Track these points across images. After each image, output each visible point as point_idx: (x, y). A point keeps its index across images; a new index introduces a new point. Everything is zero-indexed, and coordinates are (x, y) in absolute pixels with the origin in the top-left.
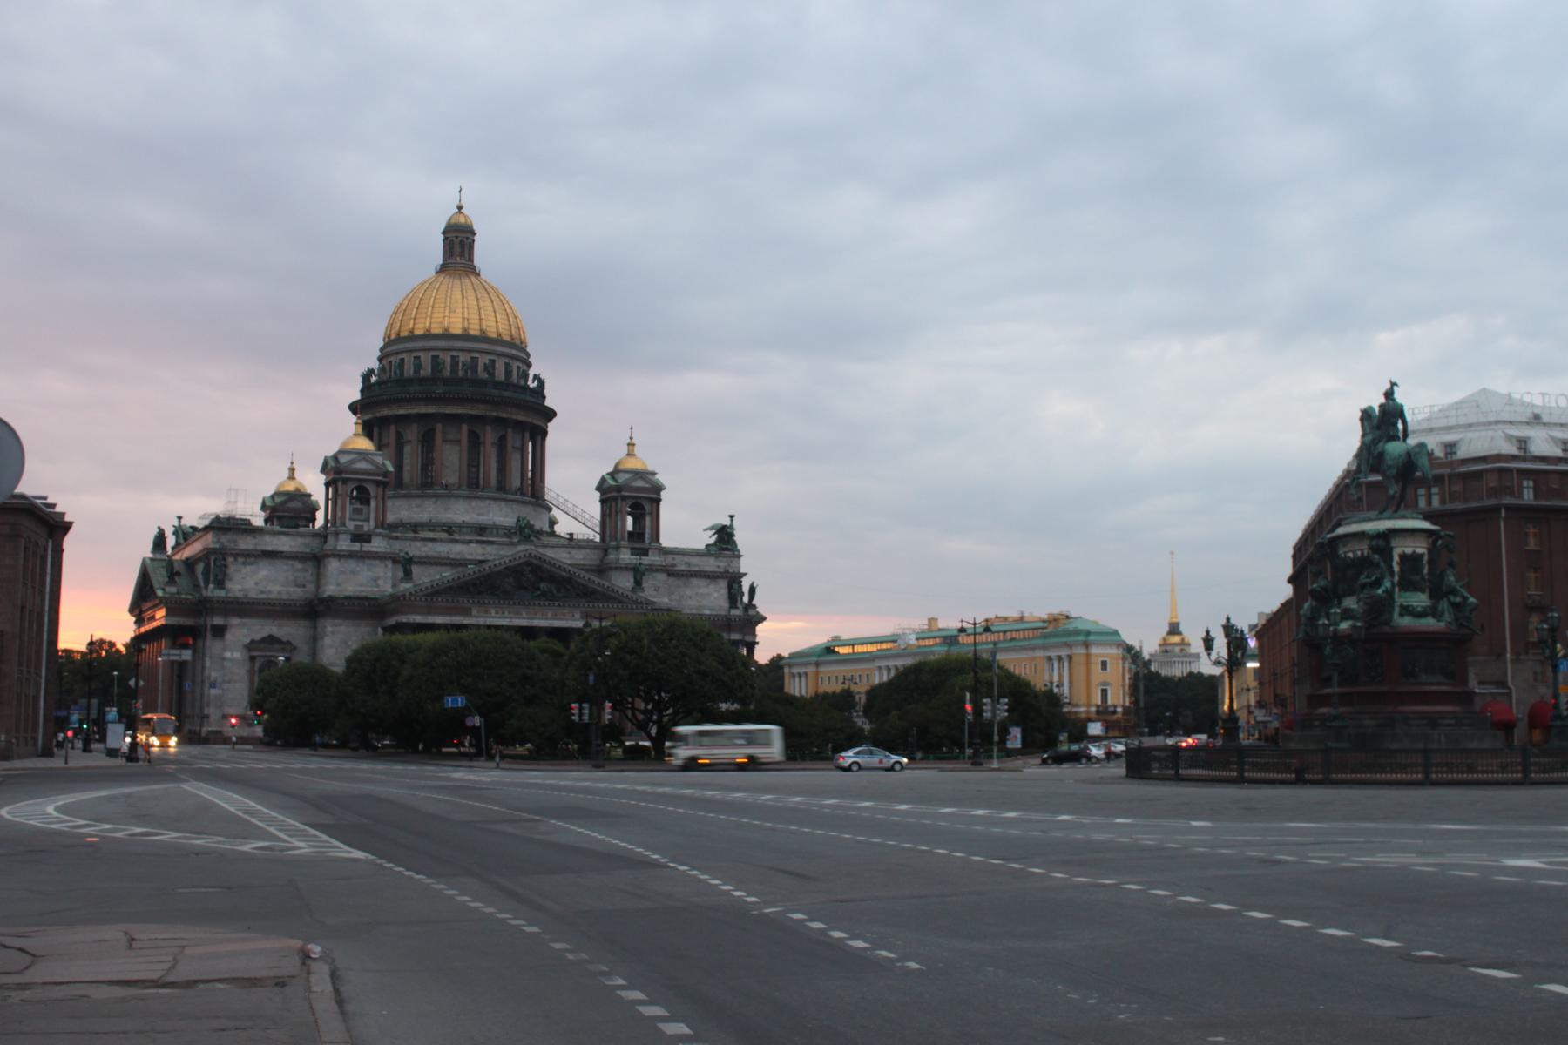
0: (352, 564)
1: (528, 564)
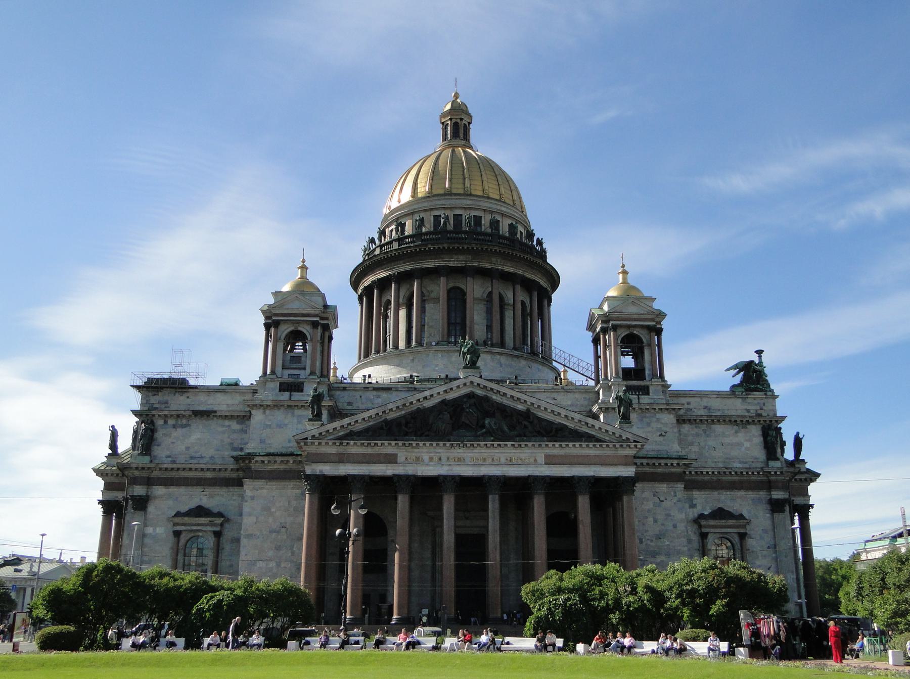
1: (471, 395)
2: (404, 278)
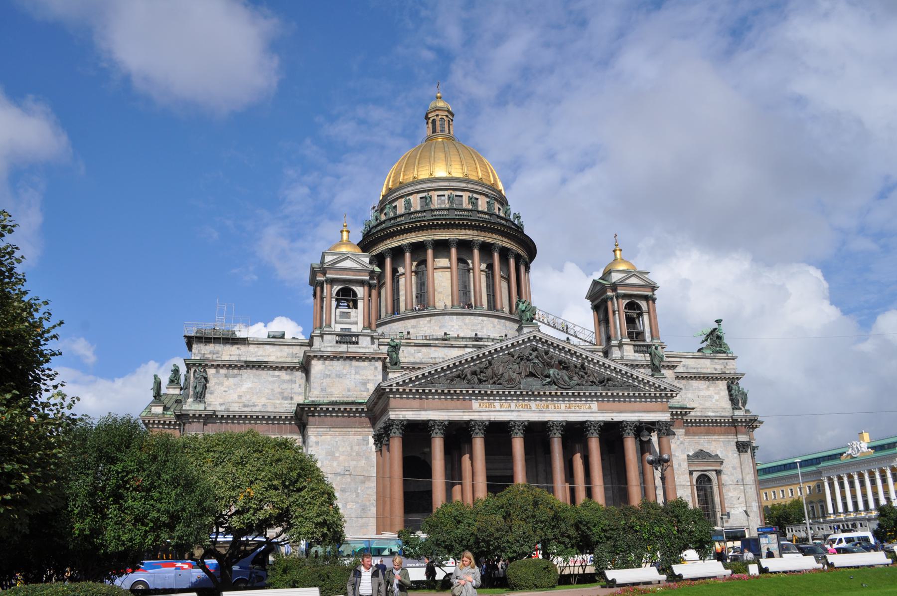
0: (337, 365)
2: (418, 249)
